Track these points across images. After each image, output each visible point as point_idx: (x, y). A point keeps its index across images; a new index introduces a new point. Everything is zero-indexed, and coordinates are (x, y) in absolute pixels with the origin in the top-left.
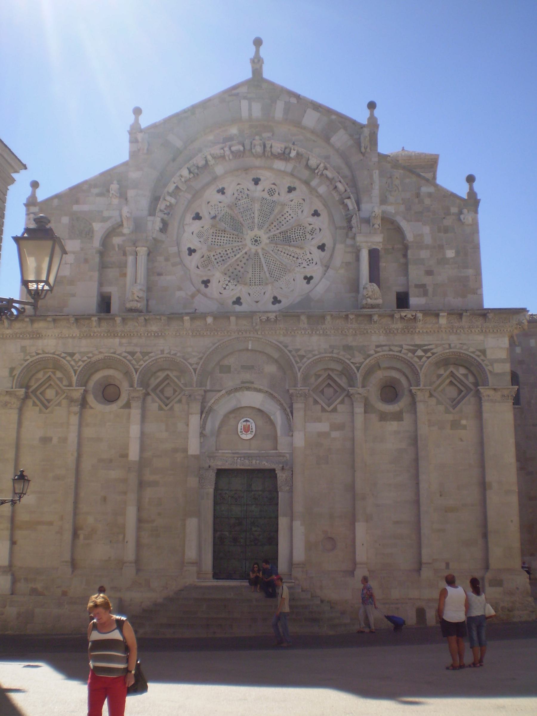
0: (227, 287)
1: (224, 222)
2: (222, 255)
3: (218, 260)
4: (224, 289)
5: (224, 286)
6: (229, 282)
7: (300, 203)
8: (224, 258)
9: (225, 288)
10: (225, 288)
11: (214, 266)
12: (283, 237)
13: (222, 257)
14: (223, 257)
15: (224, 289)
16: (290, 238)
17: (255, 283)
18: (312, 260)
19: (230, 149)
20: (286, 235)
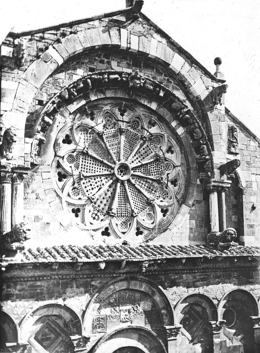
0: (96, 217)
1: (93, 149)
2: (91, 183)
3: (88, 188)
4: (94, 219)
5: (94, 216)
6: (98, 211)
7: (158, 140)
8: (93, 186)
9: (94, 218)
10: (94, 218)
11: (84, 194)
12: (144, 169)
13: (91, 185)
14: (93, 185)
15: (94, 219)
16: (150, 171)
17: (121, 214)
18: (167, 194)
19: (108, 78)
20: (146, 168)
